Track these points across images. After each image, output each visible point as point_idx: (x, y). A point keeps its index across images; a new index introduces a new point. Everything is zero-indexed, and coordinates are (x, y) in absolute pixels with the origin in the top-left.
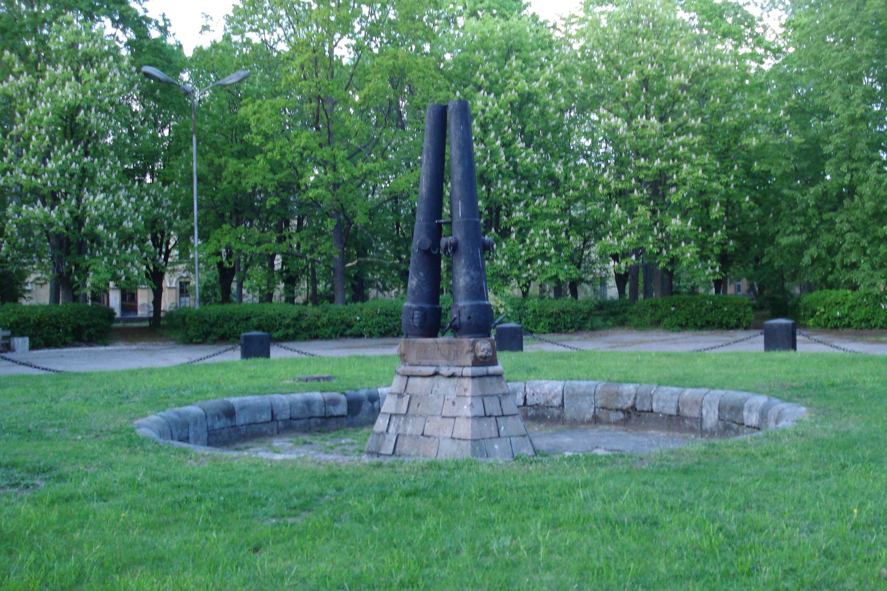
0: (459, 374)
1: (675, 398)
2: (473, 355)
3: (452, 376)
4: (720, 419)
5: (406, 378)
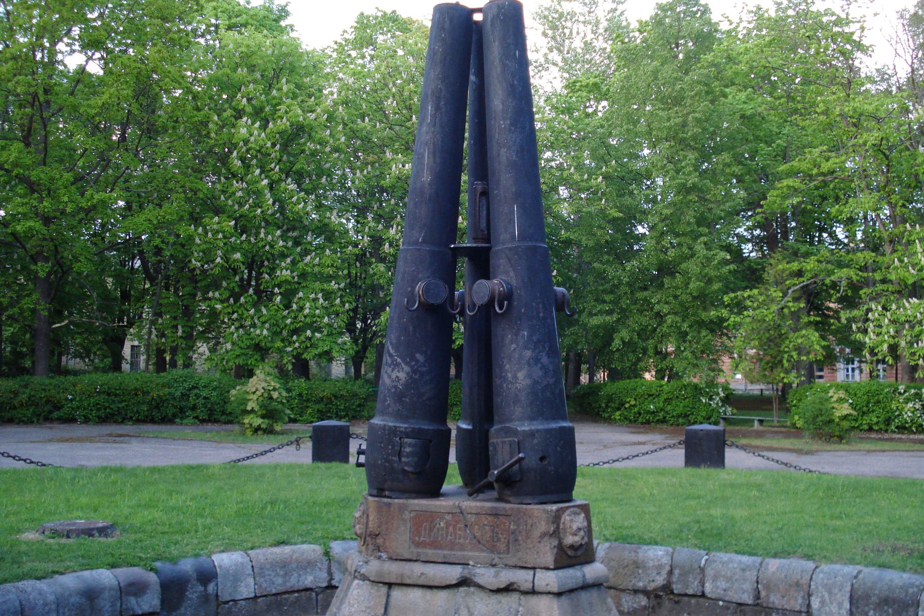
0: (527, 586)
1: (752, 575)
2: (556, 543)
3: (508, 589)
5: (384, 589)
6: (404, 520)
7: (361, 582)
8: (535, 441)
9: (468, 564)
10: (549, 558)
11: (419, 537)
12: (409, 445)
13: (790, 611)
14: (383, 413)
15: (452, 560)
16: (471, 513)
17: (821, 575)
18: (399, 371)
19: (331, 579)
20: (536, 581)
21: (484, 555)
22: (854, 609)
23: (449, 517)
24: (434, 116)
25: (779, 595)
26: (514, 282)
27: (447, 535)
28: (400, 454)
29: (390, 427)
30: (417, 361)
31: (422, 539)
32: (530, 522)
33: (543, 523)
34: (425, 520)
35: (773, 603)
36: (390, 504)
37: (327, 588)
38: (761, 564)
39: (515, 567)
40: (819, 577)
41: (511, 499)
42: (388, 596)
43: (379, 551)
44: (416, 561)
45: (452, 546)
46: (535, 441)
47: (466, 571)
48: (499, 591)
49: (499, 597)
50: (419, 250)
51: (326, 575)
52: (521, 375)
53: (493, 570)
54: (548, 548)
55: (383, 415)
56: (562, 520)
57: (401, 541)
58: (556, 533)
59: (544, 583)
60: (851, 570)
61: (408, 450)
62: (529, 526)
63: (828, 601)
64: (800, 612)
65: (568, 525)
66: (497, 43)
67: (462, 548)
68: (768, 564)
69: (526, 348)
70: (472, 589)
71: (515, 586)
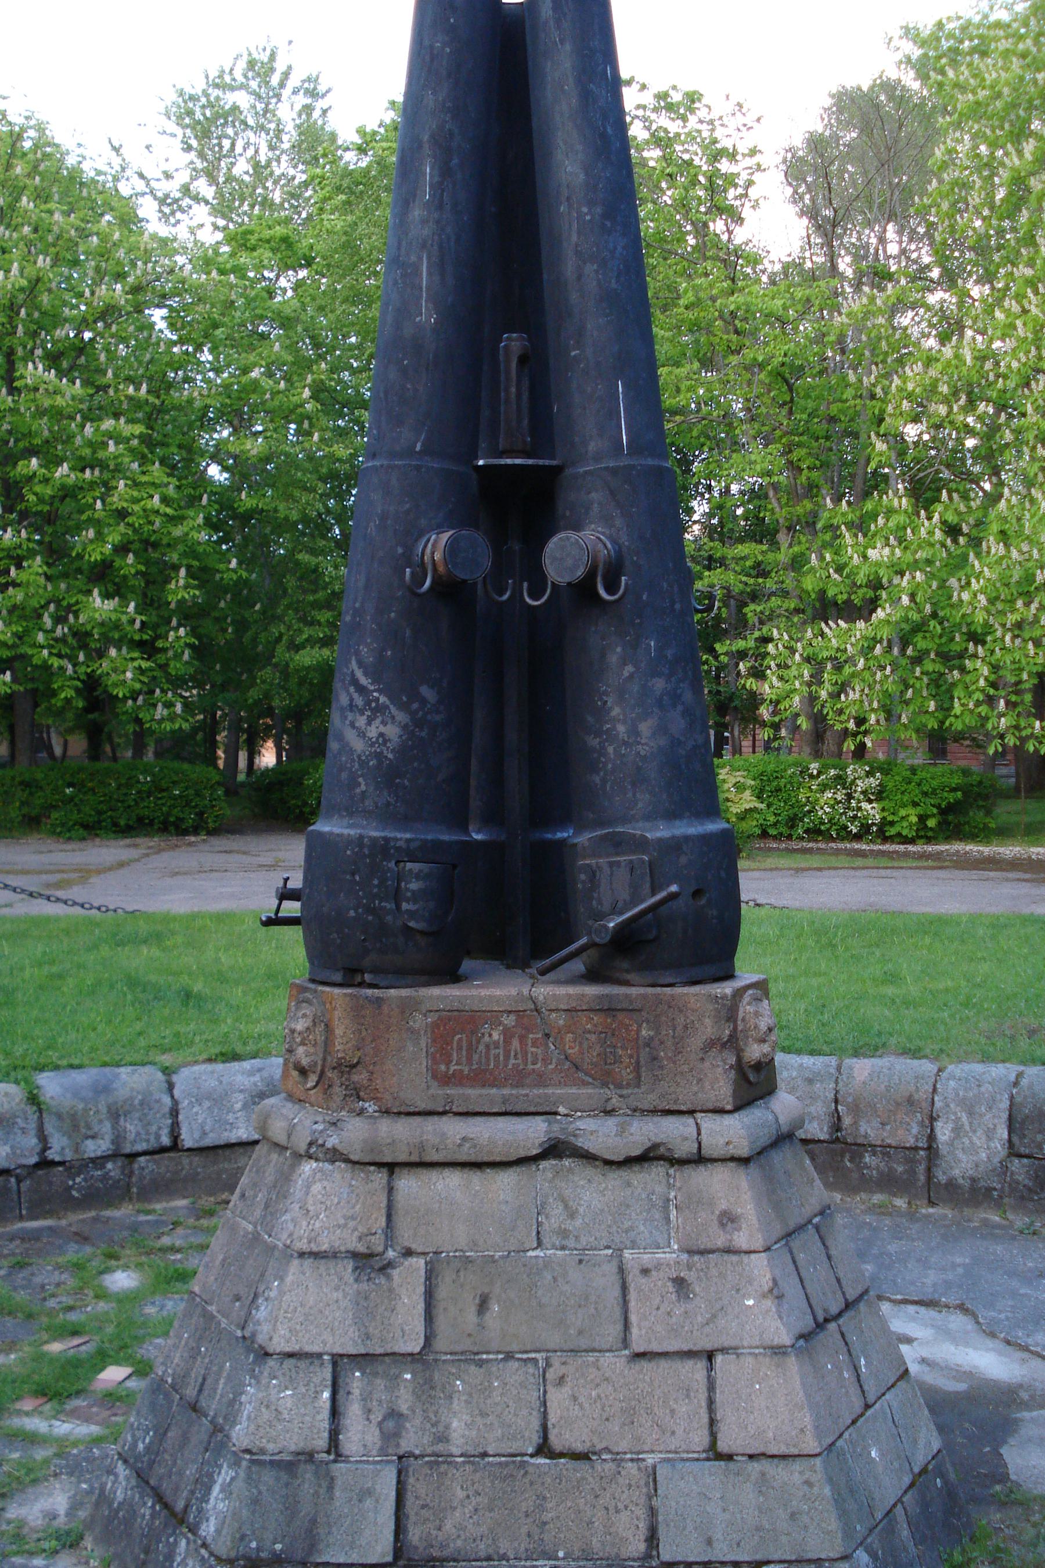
0: (686, 1149)
1: (825, 1090)
2: (732, 1060)
3: (647, 1157)
4: (1013, 1152)
5: (380, 1178)
6: (412, 1031)
7: (327, 1166)
8: (683, 860)
9: (556, 1113)
10: (720, 1086)
11: (448, 1063)
12: (418, 876)
13: (896, 1148)
14: (350, 810)
15: (518, 1108)
16: (557, 1010)
17: (952, 1083)
18: (384, 723)
19: (45, 1148)
20: (704, 1137)
21: (590, 1093)
22: (1015, 1139)
23: (509, 1021)
24: (438, 188)
25: (875, 1123)
26: (624, 540)
27: (507, 1057)
28: (397, 896)
29: (374, 840)
30: (424, 701)
31: (453, 1068)
32: (681, 1020)
33: (707, 1021)
34: (456, 1028)
35: (866, 1136)
36: (379, 1001)
37: (37, 1166)
38: (839, 1068)
39: (654, 1112)
40: (949, 1086)
41: (629, 977)
42: (391, 1190)
43: (359, 1098)
44: (444, 1113)
45: (519, 1078)
46: (683, 860)
47: (556, 1127)
48: (629, 1162)
49: (624, 1174)
50: (418, 468)
51: (34, 1141)
52: (645, 728)
53: (611, 1122)
54: (720, 1070)
55: (351, 815)
56: (741, 1015)
57: (409, 1073)
58: (733, 1043)
59: (722, 1141)
60: (1003, 1072)
61: (414, 886)
62: (679, 1028)
63: (967, 1128)
64: (916, 1149)
65: (752, 1023)
66: (568, 47)
67: (541, 1080)
68: (851, 1068)
69: (655, 674)
70: (567, 1162)
71: (662, 1150)
